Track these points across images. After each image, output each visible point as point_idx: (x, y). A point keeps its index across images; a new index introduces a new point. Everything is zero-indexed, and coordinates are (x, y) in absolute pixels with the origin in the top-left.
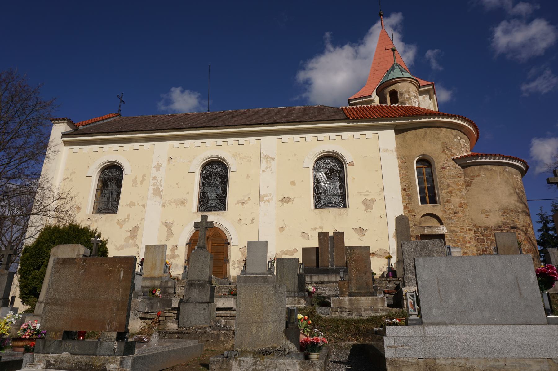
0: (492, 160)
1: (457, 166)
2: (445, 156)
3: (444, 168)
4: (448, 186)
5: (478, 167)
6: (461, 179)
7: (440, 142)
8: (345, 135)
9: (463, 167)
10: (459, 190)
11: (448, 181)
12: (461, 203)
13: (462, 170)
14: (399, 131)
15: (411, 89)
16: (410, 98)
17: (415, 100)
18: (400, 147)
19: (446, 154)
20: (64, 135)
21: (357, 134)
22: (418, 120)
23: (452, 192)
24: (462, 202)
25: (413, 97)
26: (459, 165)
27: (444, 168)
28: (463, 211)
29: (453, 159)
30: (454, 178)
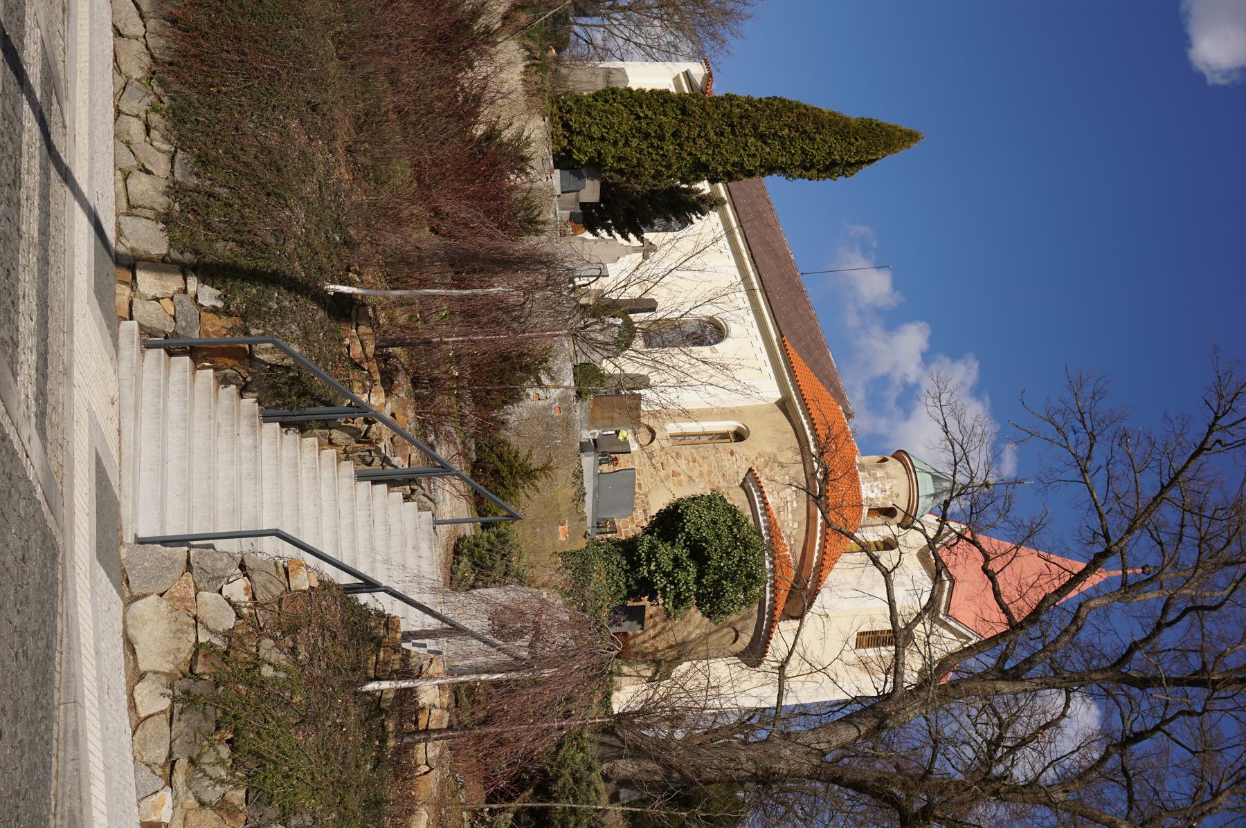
0: (759, 512)
1: (742, 476)
2: (753, 458)
3: (732, 453)
4: (704, 458)
5: (746, 499)
6: (721, 480)
7: (775, 451)
8: (760, 343)
9: (742, 486)
10: (701, 474)
11: (712, 458)
12: (680, 475)
13: (737, 484)
14: (784, 405)
15: (895, 482)
16: (876, 479)
17: (876, 490)
18: (758, 411)
19: (757, 458)
20: (687, 74)
21: (764, 356)
22: (802, 416)
23: (694, 461)
24: (682, 477)
25: (880, 486)
26: (744, 480)
27: (732, 453)
28: (667, 477)
29: (750, 470)
30: (720, 468)
